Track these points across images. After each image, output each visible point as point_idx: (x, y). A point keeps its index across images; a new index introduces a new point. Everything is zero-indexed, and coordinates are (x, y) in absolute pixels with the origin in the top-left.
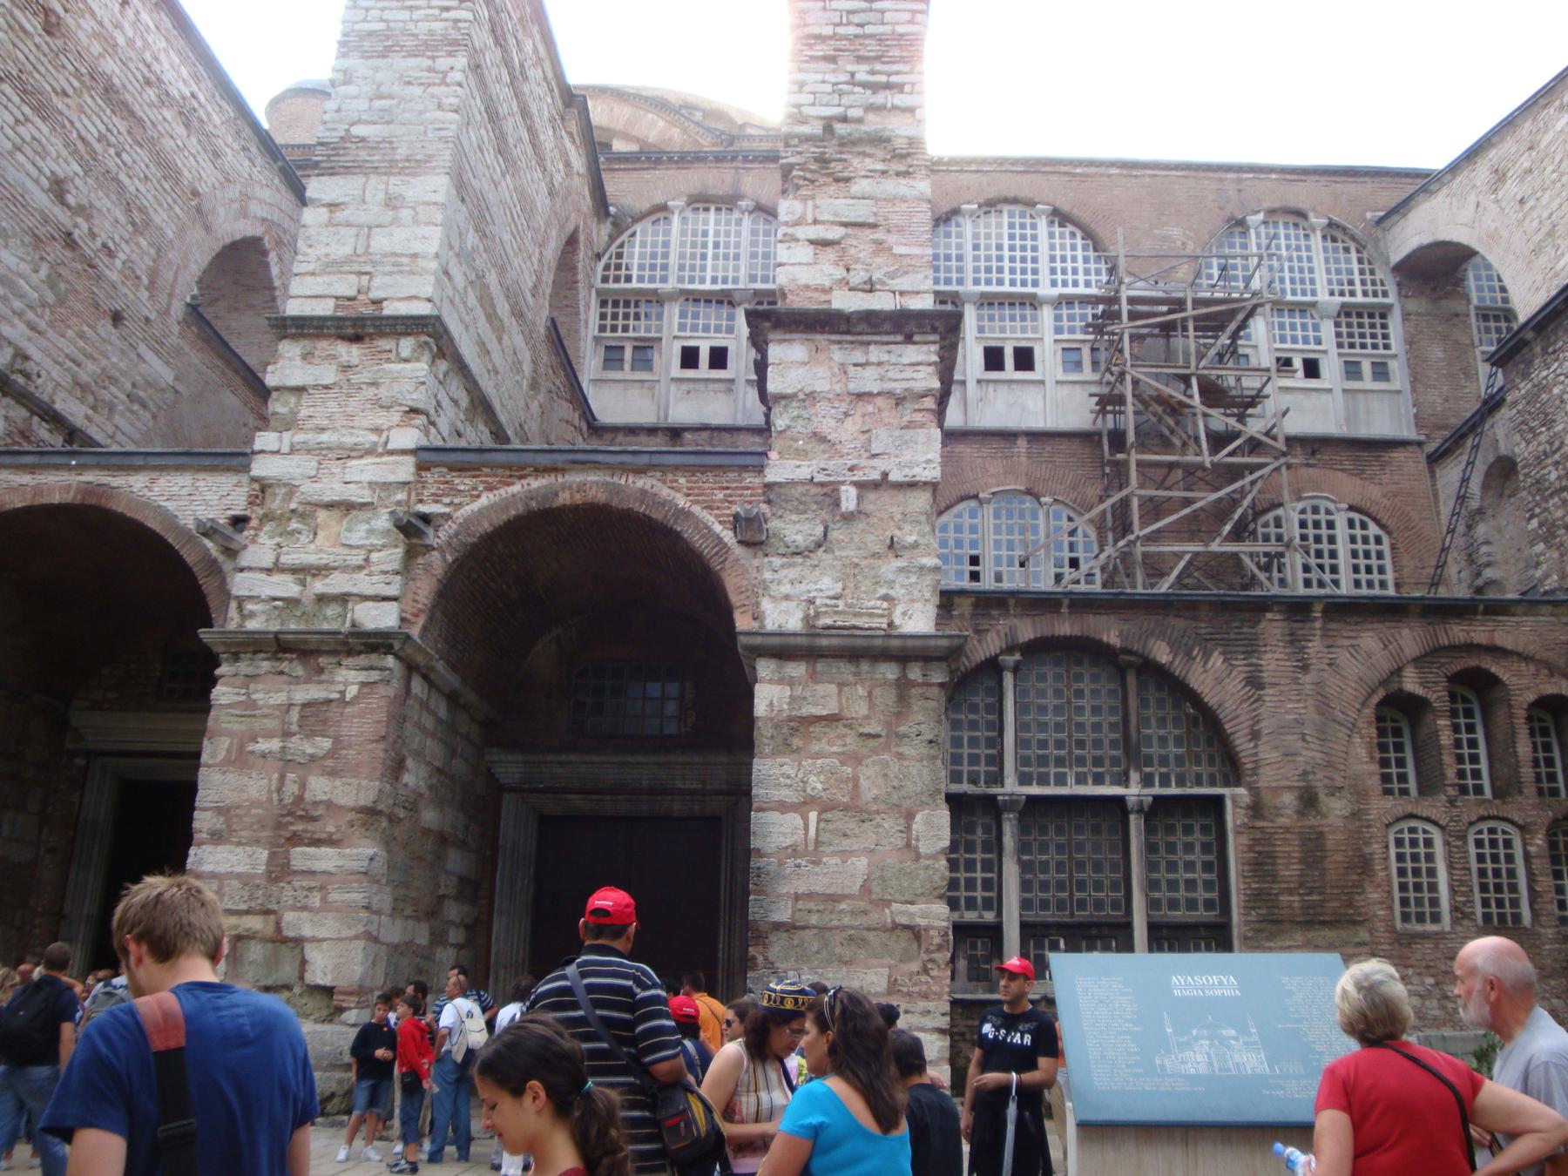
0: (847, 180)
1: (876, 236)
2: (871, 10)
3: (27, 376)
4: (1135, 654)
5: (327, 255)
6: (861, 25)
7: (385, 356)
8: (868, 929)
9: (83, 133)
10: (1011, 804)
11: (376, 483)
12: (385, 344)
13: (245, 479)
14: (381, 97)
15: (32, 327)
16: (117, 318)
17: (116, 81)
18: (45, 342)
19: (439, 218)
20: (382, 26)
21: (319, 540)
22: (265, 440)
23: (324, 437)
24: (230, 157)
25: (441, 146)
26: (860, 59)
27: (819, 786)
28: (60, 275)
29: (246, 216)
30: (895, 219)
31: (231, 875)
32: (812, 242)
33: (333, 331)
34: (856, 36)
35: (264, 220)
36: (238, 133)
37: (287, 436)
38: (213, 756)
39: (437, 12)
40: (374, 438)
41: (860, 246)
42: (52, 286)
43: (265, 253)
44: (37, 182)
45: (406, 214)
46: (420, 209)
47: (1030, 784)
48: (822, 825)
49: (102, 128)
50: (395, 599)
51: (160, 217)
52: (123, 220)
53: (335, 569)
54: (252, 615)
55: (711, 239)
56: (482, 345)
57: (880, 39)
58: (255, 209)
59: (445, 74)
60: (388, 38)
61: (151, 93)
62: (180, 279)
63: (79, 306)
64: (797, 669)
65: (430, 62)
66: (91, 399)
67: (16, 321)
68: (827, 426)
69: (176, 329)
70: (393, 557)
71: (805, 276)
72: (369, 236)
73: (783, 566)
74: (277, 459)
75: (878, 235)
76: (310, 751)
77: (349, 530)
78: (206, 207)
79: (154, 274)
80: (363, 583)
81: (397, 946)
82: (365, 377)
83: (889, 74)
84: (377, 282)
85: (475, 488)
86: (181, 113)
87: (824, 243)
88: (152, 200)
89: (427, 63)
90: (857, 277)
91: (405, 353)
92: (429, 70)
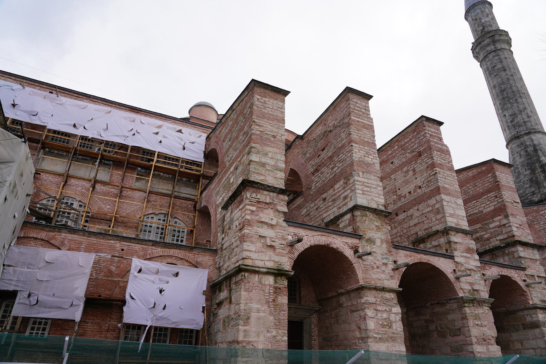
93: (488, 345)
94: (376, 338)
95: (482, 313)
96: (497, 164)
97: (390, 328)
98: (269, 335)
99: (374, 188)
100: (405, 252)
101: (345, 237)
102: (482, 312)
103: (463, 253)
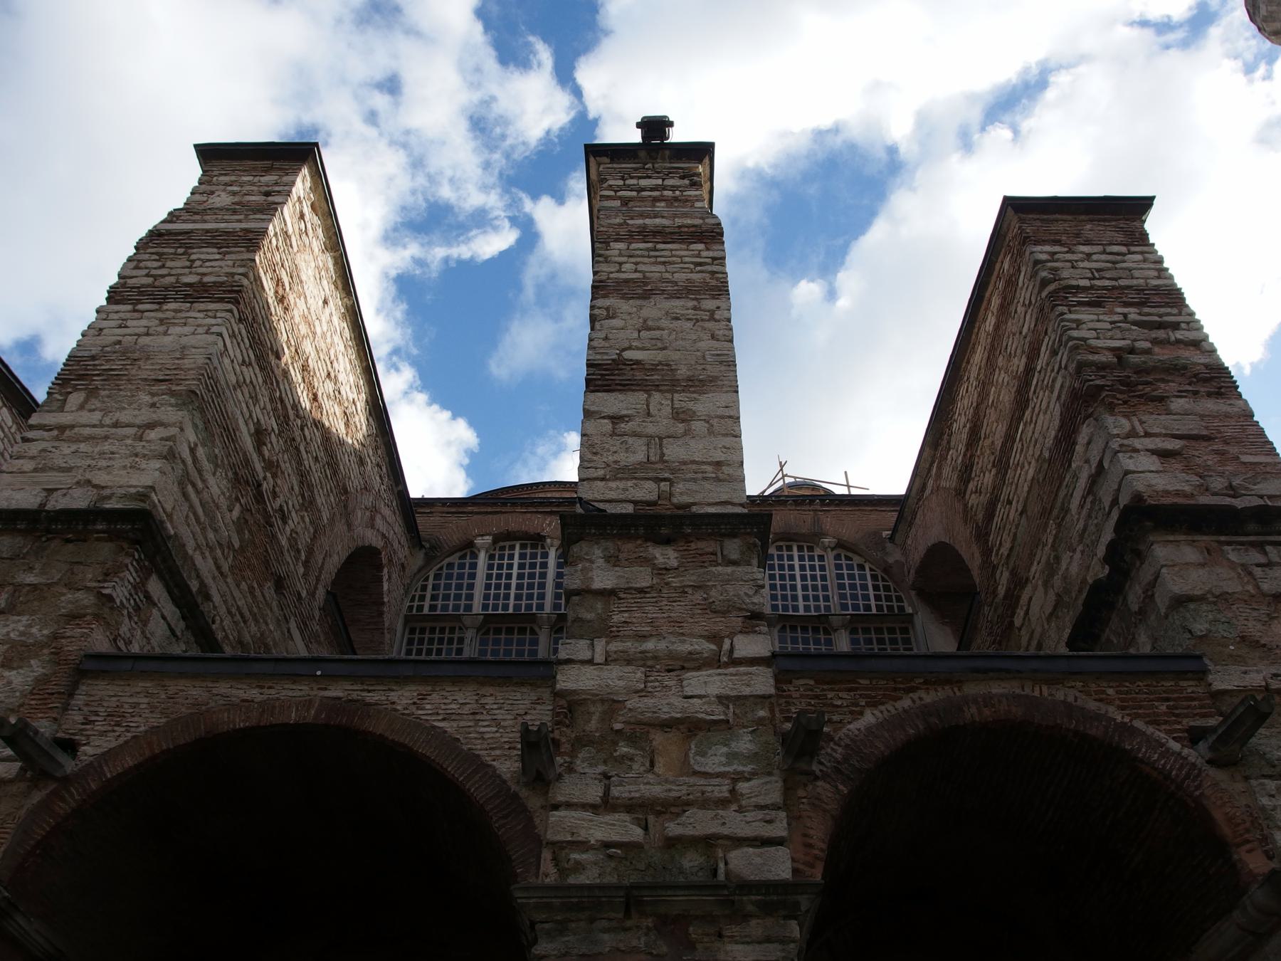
0: (1161, 399)
1: (1215, 447)
2: (1116, 269)
5: (616, 462)
6: (1116, 279)
7: (706, 558)
9: (284, 395)
11: (728, 698)
12: (708, 546)
13: (546, 694)
14: (649, 329)
15: (219, 568)
16: (280, 584)
18: (225, 588)
21: (655, 769)
22: (577, 648)
23: (650, 645)
24: (369, 468)
25: (723, 368)
26: (1126, 305)
28: (246, 521)
29: (373, 527)
30: (1229, 432)
32: (1154, 452)
33: (641, 531)
34: (1114, 288)
35: (383, 536)
36: (377, 448)
37: (600, 645)
39: (692, 266)
40: (713, 647)
41: (1204, 455)
42: (240, 532)
43: (380, 567)
45: (698, 426)
46: (715, 422)
50: (778, 842)
51: (320, 500)
52: (296, 488)
53: (689, 804)
54: (579, 867)
55: (797, 573)
57: (1139, 290)
58: (379, 521)
59: (712, 312)
60: (646, 284)
61: (329, 386)
62: (326, 566)
63: (254, 561)
65: (695, 303)
67: (207, 554)
68: (1254, 629)
69: (317, 614)
70: (768, 789)
72: (661, 445)
74: (589, 670)
75: (1218, 446)
77: (704, 755)
78: (350, 506)
79: (310, 552)
80: (735, 823)
82: (690, 578)
83: (1160, 316)
84: (680, 487)
85: (857, 705)
86: (345, 413)
87: (1164, 455)
88: (317, 478)
89: (691, 304)
90: (1218, 483)
91: (735, 556)
92: (695, 308)
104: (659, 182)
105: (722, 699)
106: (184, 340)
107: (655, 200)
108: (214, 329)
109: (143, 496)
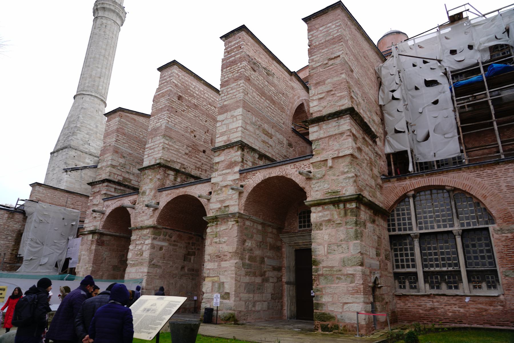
3: (185, 168)
4: (450, 186)
8: (341, 275)
10: (416, 236)
16: (204, 152)
17: (196, 104)
19: (241, 118)
20: (228, 78)
22: (214, 175)
27: (327, 238)
31: (212, 269)
37: (216, 173)
38: (207, 243)
44: (181, 130)
47: (422, 229)
48: (329, 248)
49: (194, 114)
56: (264, 142)
64: (320, 209)
66: (200, 170)
71: (316, 109)
73: (316, 183)
76: (224, 240)
81: (248, 283)
88: (209, 125)
93: (222, 261)
94: (131, 264)
95: (224, 229)
96: (313, 20)
97: (141, 256)
98: (85, 267)
99: (157, 147)
100: (167, 192)
101: (130, 197)
102: (226, 228)
103: (223, 171)
104: (235, 42)
105: (232, 181)
106: (162, 123)
107: (234, 49)
108: (165, 119)
109: (161, 159)
